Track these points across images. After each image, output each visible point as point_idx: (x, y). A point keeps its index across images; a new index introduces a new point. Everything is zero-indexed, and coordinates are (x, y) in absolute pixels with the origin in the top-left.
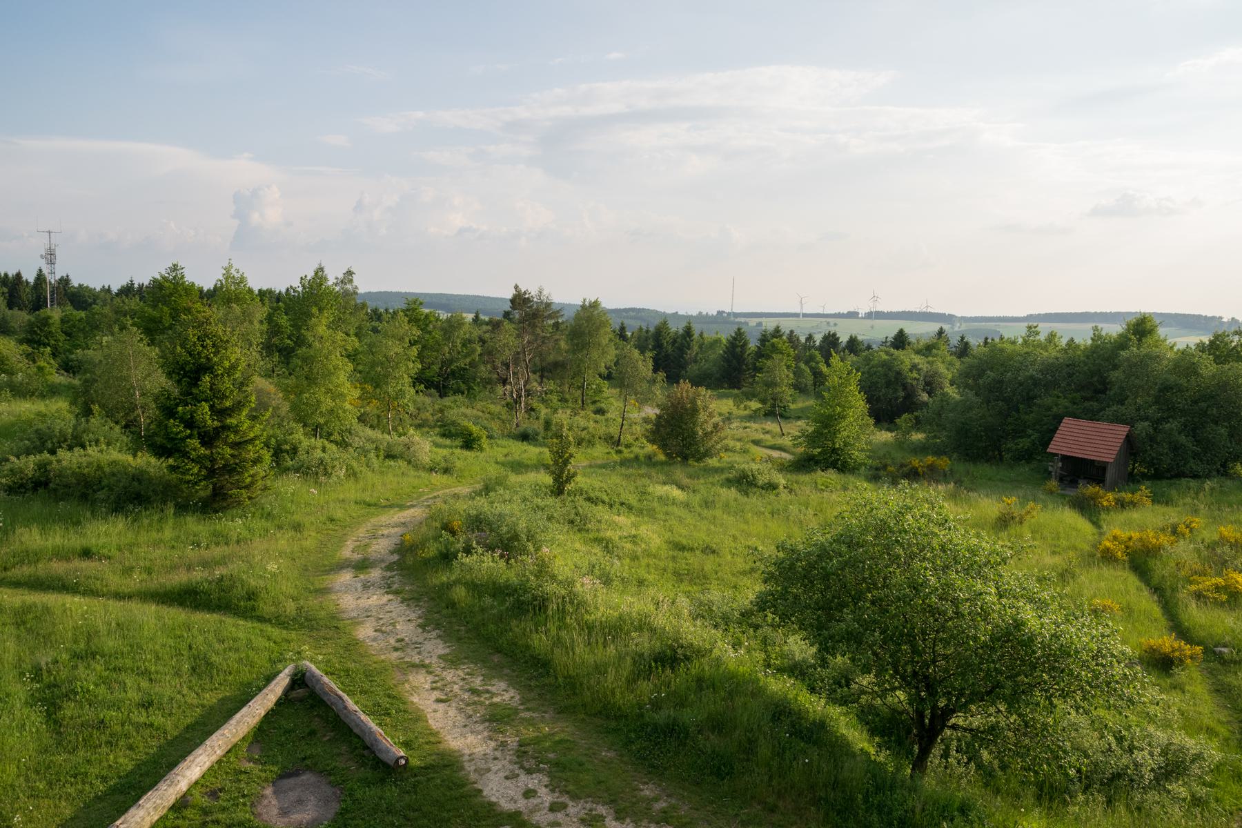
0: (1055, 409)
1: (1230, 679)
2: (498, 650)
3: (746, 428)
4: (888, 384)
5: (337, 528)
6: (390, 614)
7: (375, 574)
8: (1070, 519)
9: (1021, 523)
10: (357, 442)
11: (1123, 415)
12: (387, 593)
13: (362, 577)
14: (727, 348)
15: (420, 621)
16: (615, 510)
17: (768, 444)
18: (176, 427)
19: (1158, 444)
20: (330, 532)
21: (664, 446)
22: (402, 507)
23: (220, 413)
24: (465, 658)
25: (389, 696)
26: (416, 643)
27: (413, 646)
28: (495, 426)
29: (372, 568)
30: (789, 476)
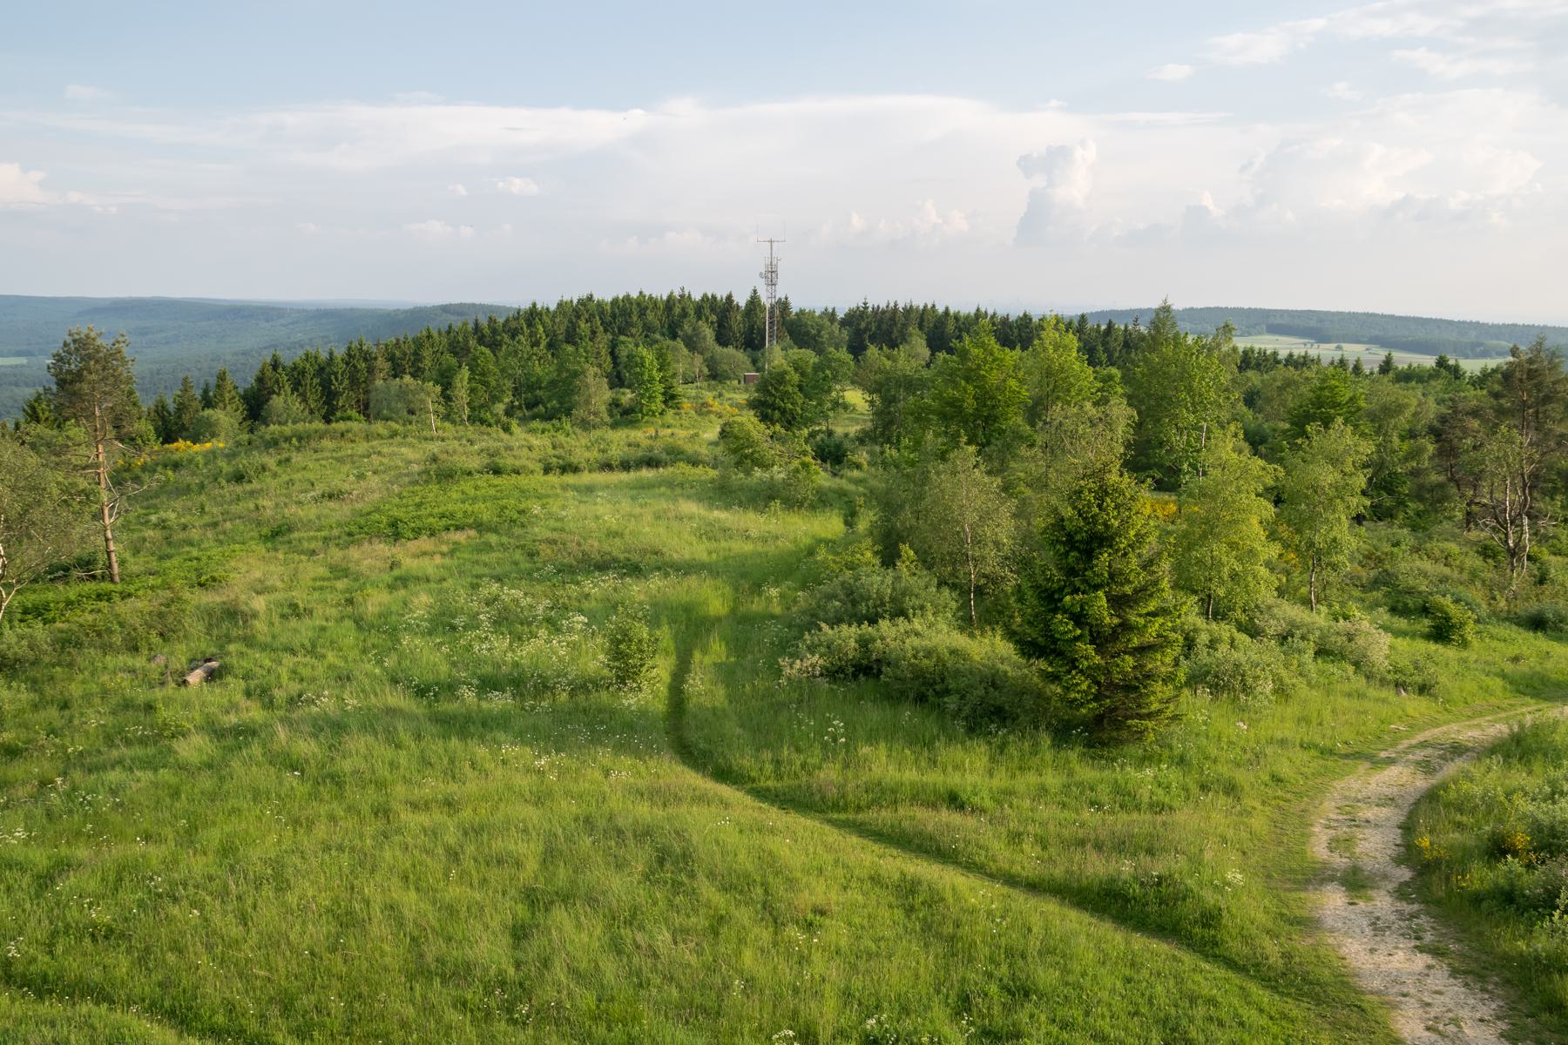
5: (1289, 796)
10: (1273, 627)
12: (1421, 949)
18: (1063, 625)
20: (1281, 803)
22: (1377, 763)
23: (1119, 603)
29: (1372, 888)
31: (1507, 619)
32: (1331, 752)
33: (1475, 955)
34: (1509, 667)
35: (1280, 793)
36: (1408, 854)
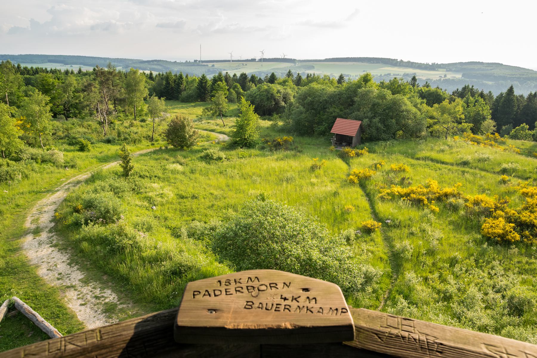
0: (334, 114)
1: (390, 234)
2: (106, 273)
3: (208, 123)
4: (268, 99)
5: (21, 210)
6: (53, 259)
7: (44, 236)
8: (339, 162)
9: (320, 168)
10: (24, 156)
11: (359, 116)
12: (51, 247)
13: (37, 238)
14: (198, 83)
15: (68, 261)
16: (152, 180)
17: (218, 131)
19: (371, 127)
20: (18, 213)
21: (172, 143)
24: (91, 279)
25: (58, 307)
26: (68, 274)
27: (66, 276)
28: (94, 136)
29: (42, 232)
30: (227, 152)
31: (101, 141)
32: (40, 192)
33: (66, 243)
34: (99, 155)
35: (18, 210)
36: (54, 220)
